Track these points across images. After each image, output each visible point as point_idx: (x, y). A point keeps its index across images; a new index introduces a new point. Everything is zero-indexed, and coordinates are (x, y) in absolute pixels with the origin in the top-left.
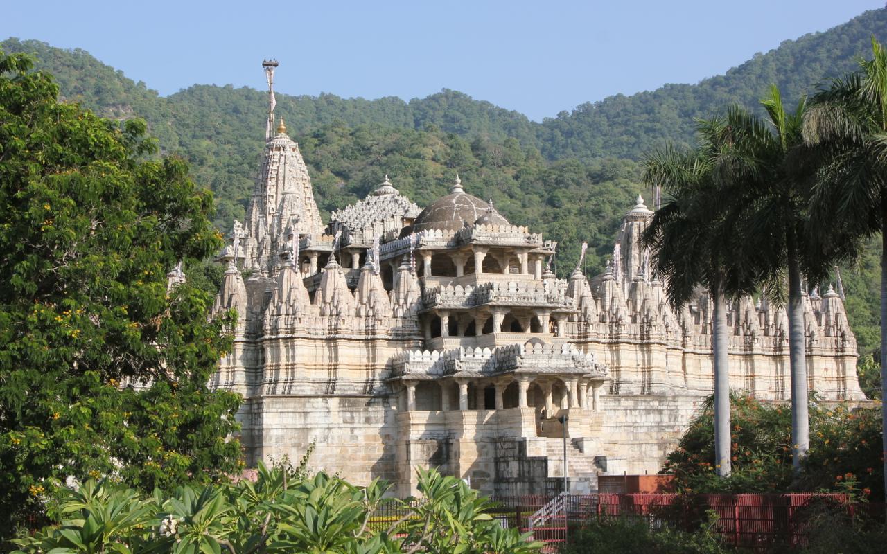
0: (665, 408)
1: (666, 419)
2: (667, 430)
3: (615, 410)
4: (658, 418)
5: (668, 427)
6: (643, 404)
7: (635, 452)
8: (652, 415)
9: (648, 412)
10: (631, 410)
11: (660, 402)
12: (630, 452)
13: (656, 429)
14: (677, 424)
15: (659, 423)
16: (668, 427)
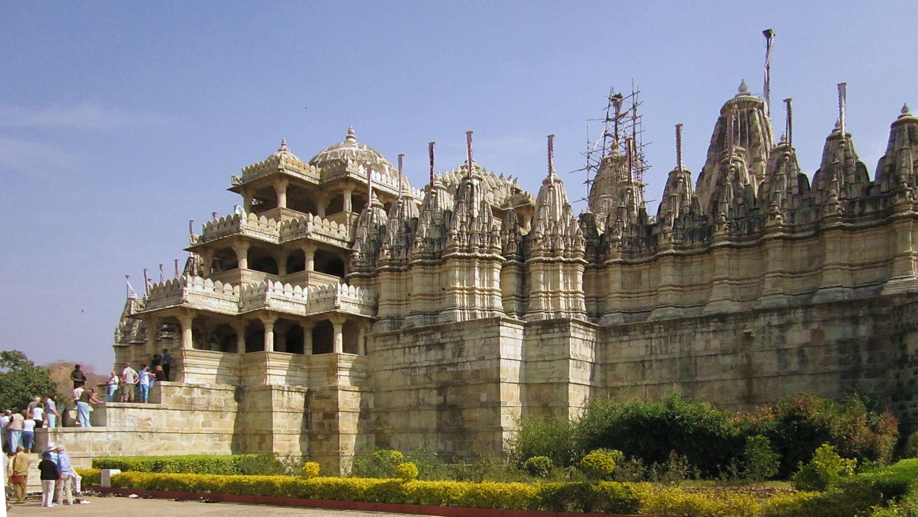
0: (447, 340)
1: (449, 354)
2: (449, 369)
3: (393, 349)
4: (439, 355)
5: (449, 365)
6: (424, 338)
7: (411, 399)
8: (433, 352)
9: (429, 348)
10: (410, 348)
11: (442, 333)
12: (408, 400)
13: (436, 369)
14: (460, 360)
15: (439, 361)
16: (449, 365)
